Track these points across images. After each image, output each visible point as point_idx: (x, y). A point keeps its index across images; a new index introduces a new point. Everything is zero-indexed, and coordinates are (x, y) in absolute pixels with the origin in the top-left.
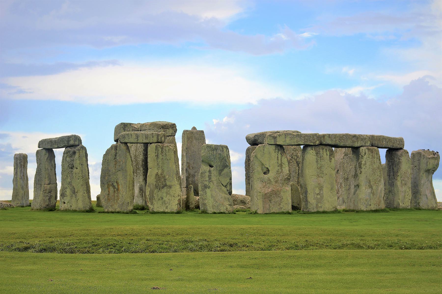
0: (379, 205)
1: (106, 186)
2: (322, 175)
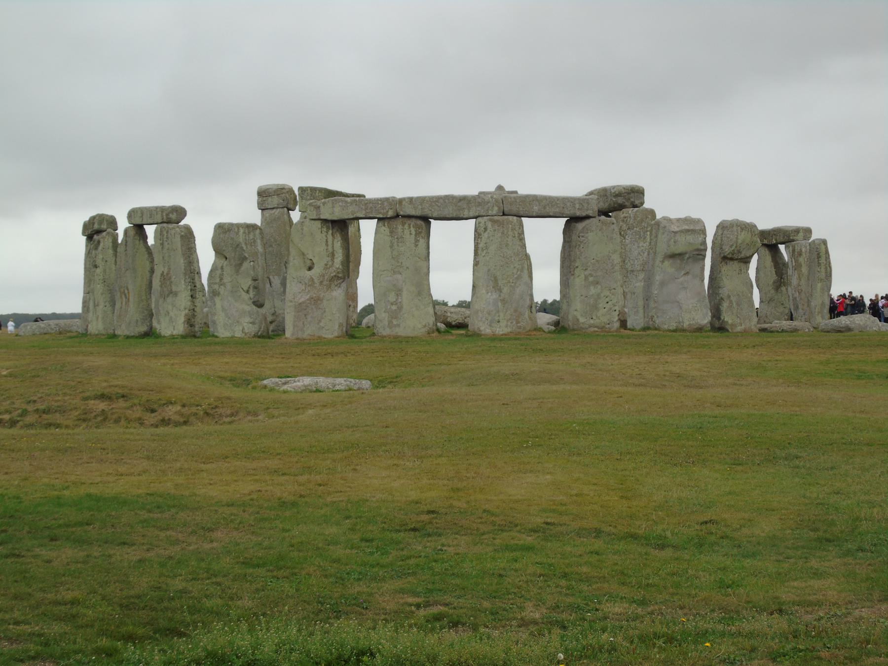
0: (518, 322)
1: (119, 294)
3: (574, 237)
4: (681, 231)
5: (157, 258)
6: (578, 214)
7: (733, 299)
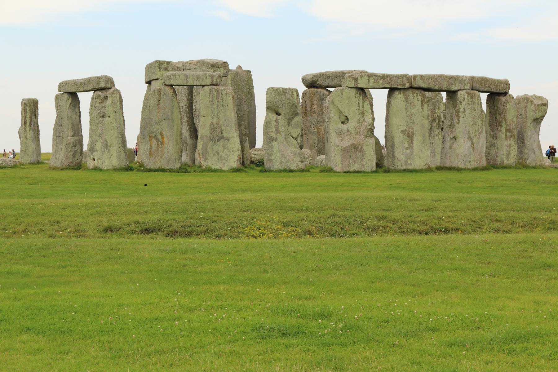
0: (480, 162)
1: (148, 138)
2: (413, 125)
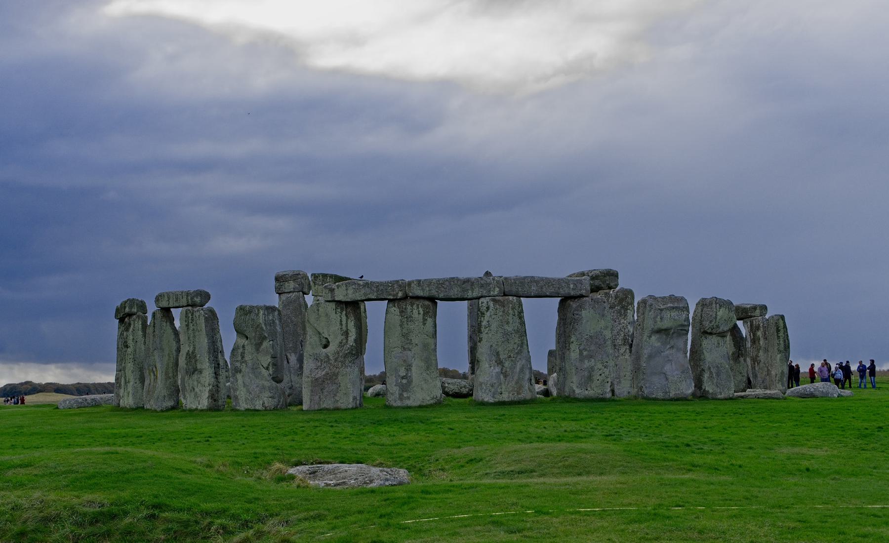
0: (518, 393)
3: (569, 315)
4: (667, 309)
5: (182, 337)
6: (572, 293)
7: (713, 370)
